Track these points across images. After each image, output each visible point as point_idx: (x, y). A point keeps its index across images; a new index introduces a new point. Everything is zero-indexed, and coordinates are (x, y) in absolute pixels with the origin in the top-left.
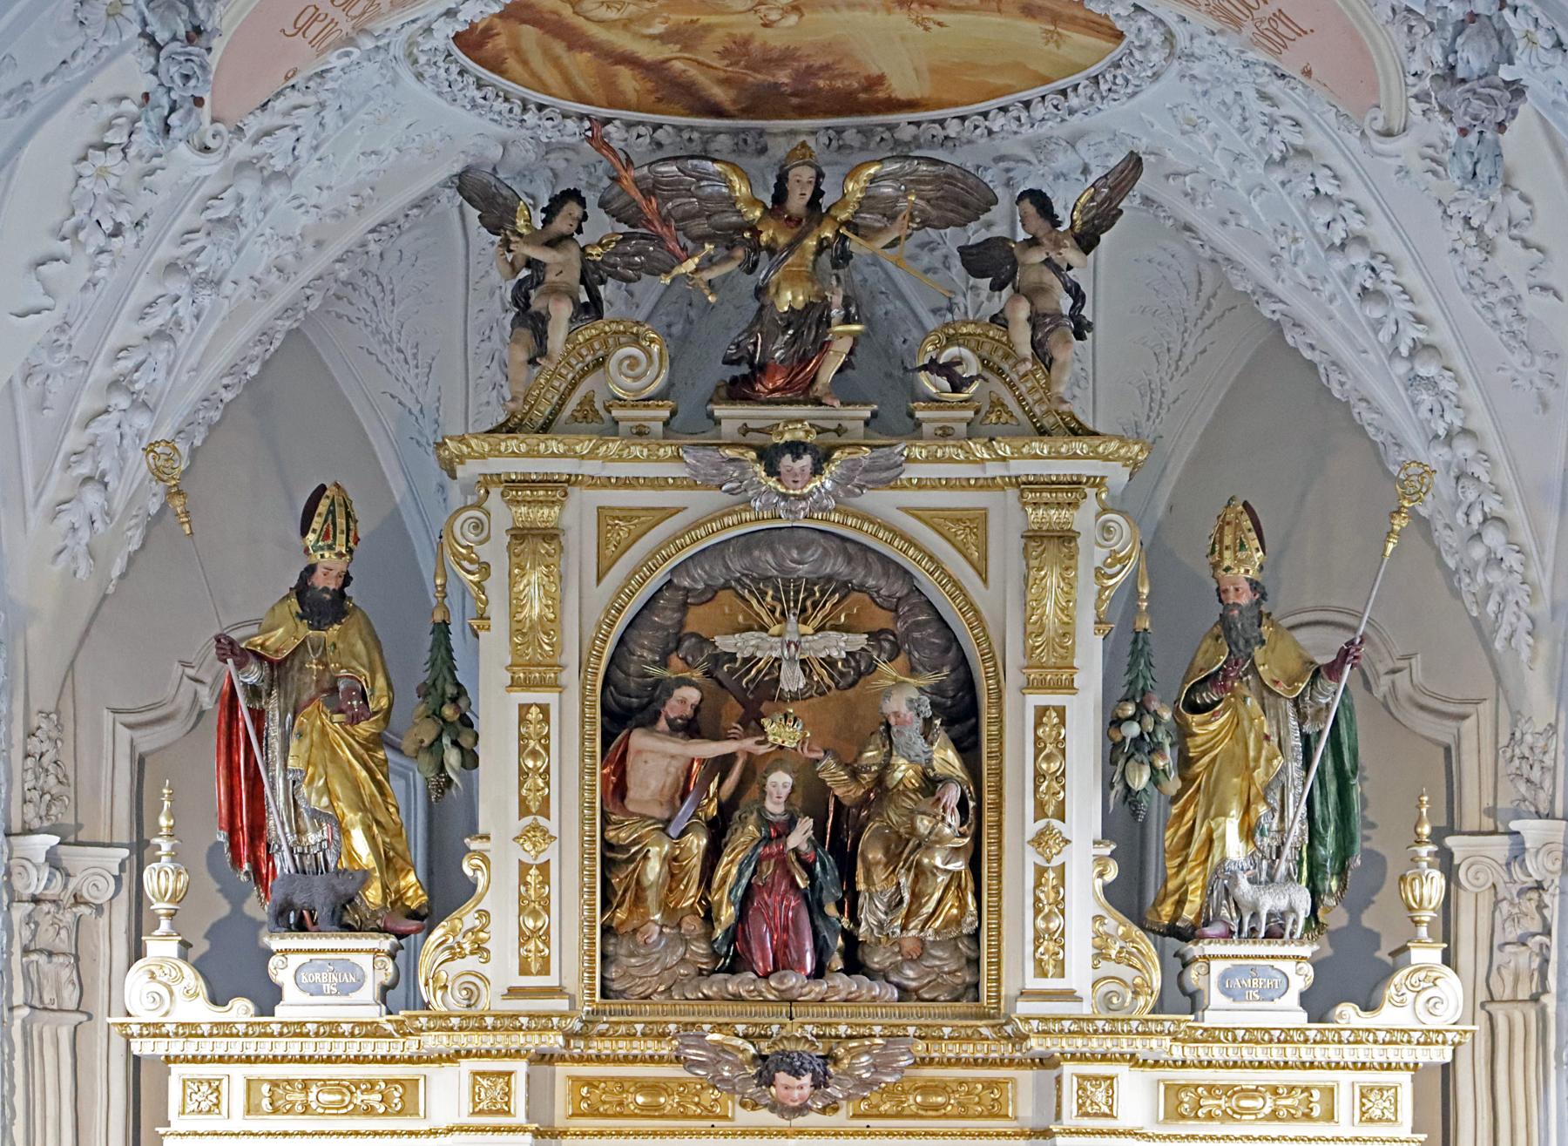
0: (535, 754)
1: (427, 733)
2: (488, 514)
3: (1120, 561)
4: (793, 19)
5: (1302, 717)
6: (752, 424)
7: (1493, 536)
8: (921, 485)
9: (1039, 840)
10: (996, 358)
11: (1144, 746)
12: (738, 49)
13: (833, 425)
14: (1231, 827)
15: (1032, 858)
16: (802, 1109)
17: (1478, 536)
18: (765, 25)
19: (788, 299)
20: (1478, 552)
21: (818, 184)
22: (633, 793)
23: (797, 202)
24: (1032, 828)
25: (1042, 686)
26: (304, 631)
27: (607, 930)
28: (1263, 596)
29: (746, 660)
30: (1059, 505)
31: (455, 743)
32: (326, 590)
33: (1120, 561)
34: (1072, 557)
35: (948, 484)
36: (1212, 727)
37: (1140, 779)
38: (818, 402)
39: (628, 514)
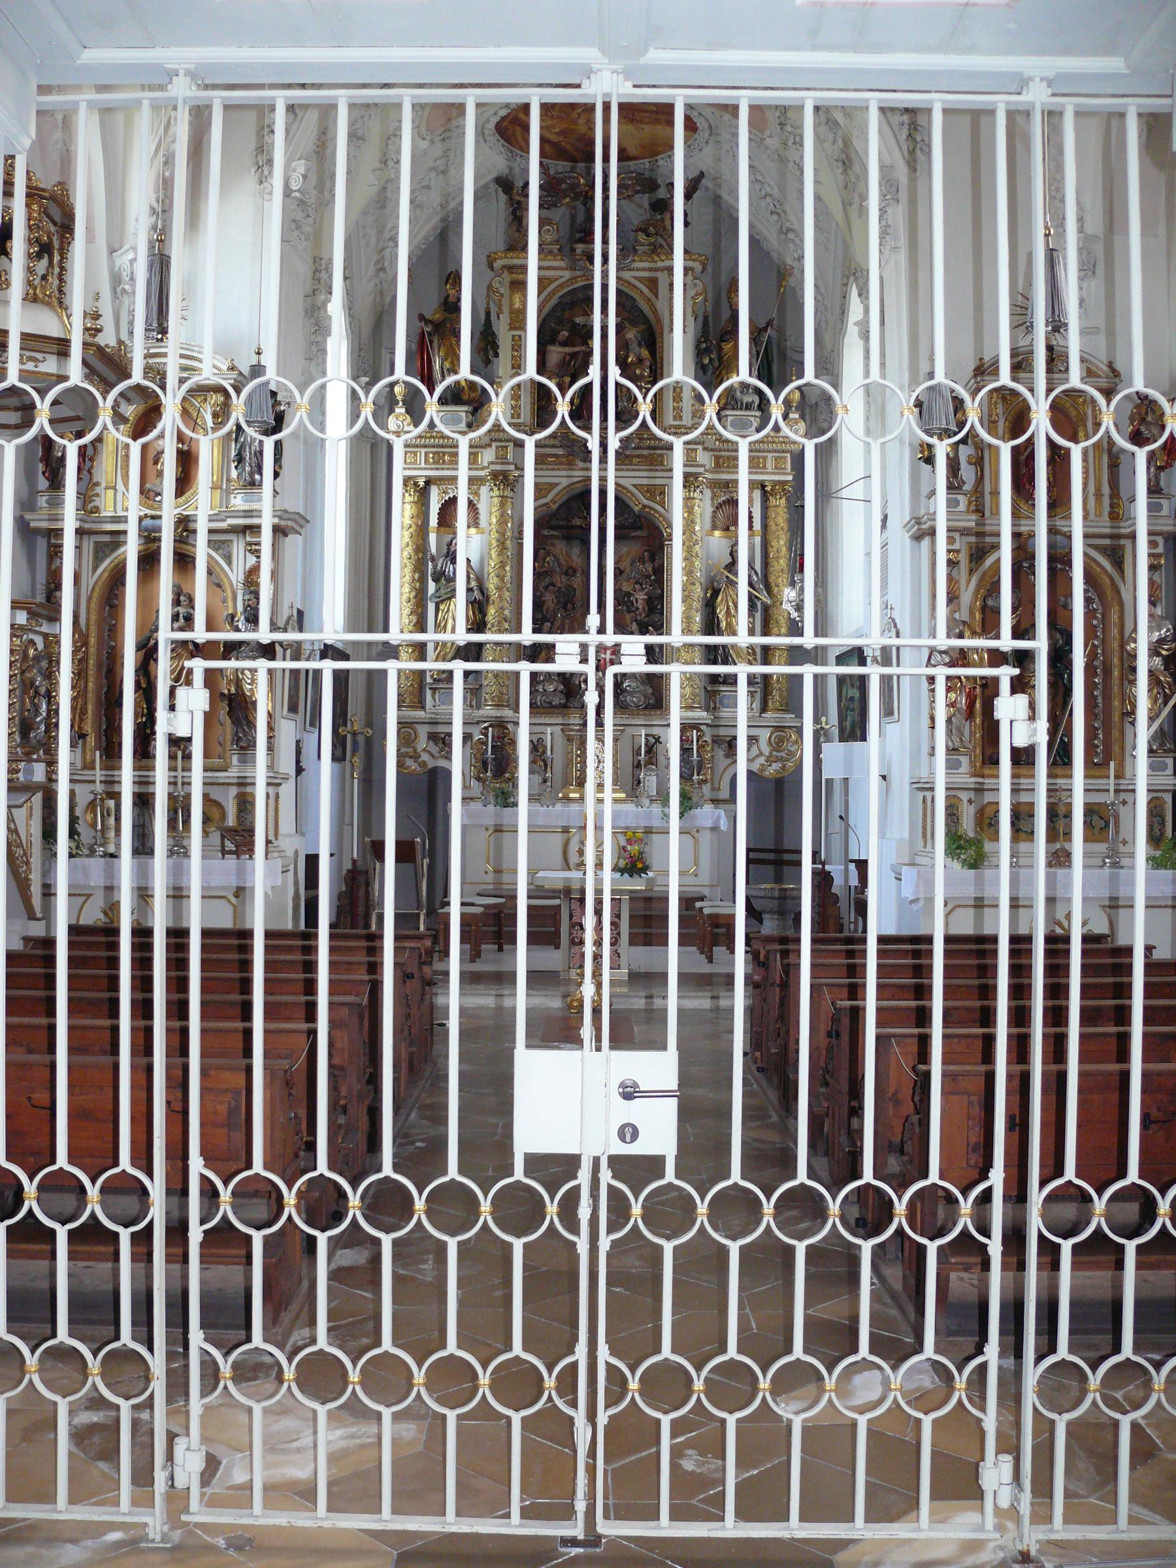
11: (707, 351)
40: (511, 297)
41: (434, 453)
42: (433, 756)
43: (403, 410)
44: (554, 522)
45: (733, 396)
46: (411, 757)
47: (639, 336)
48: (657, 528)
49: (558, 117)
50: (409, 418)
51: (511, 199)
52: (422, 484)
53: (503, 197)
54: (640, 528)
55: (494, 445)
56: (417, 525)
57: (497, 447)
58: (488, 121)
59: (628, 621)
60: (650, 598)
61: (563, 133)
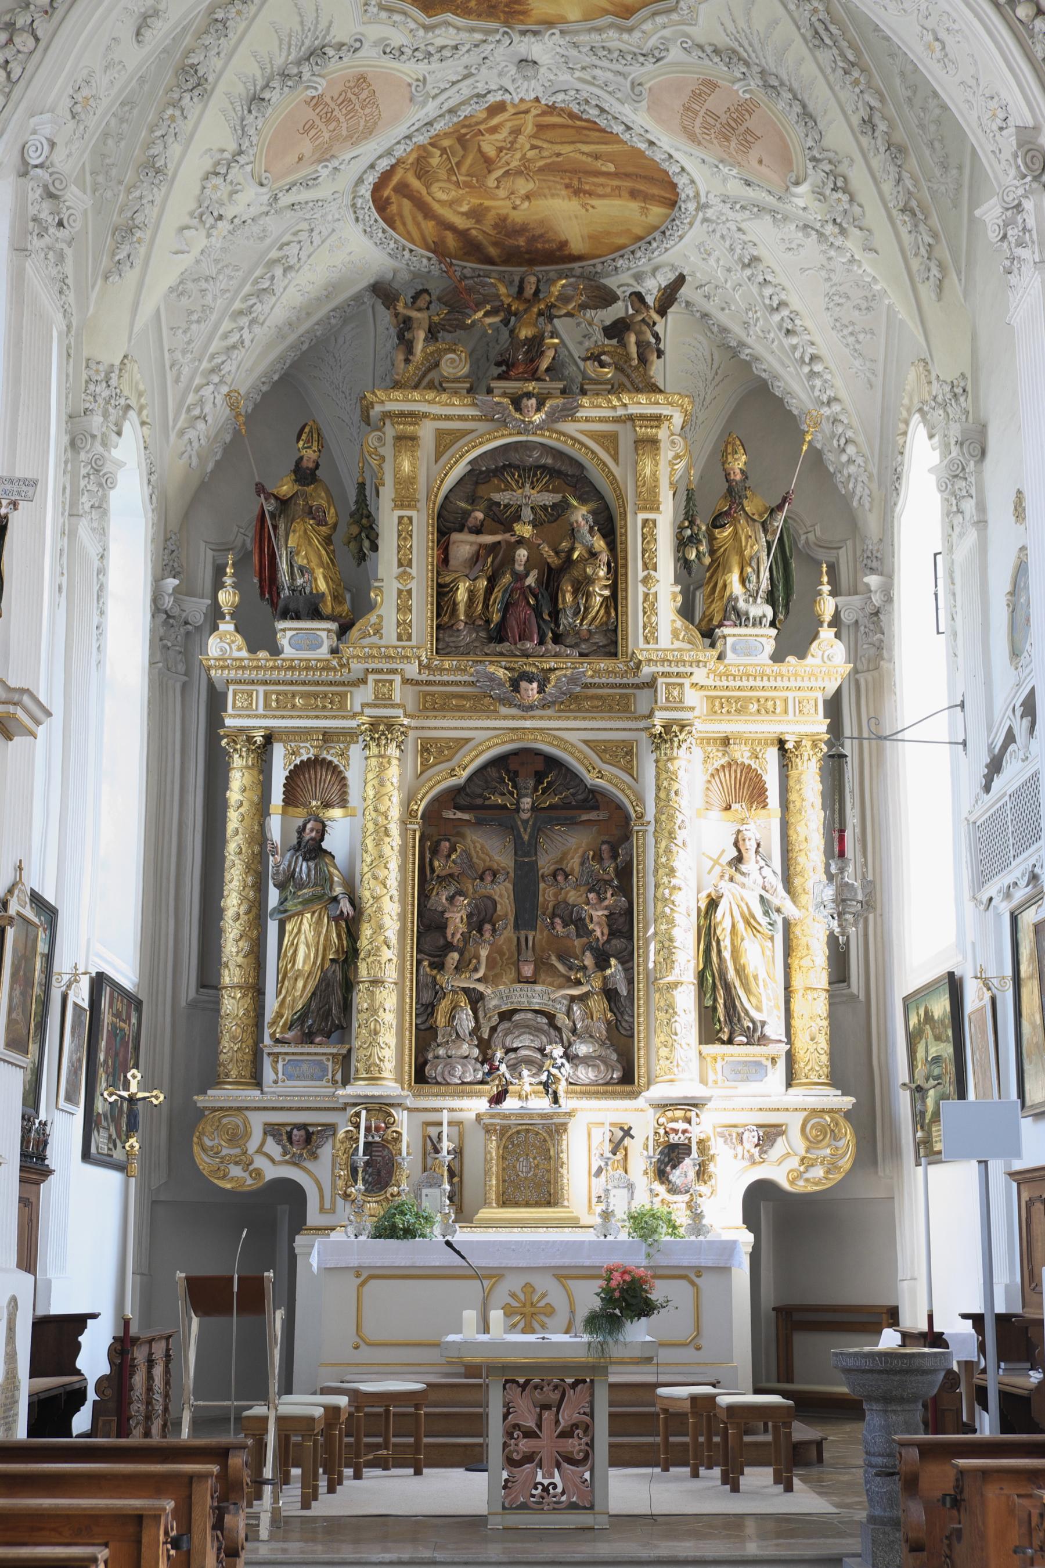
0: (405, 539)
1: (355, 530)
2: (384, 433)
3: (680, 457)
4: (526, 204)
5: (765, 531)
6: (508, 391)
7: (851, 450)
8: (587, 420)
9: (646, 580)
10: (621, 363)
11: (694, 540)
12: (501, 224)
13: (546, 391)
14: (734, 577)
15: (641, 589)
16: (531, 707)
17: (844, 450)
18: (514, 208)
19: (525, 333)
20: (844, 458)
21: (537, 287)
22: (452, 562)
23: (529, 291)
24: (641, 574)
25: (645, 509)
26: (296, 488)
27: (439, 627)
28: (747, 478)
29: (505, 506)
30: (652, 427)
31: (367, 537)
32: (307, 468)
33: (680, 457)
34: (658, 449)
35: (601, 420)
36: (726, 534)
37: (692, 556)
38: (539, 379)
39: (450, 432)
40: (395, 457)
41: (278, 694)
42: (272, 1160)
43: (231, 627)
44: (462, 801)
45: (735, 608)
46: (237, 1163)
47: (590, 518)
48: (619, 807)
49: (467, 185)
50: (239, 640)
51: (396, 315)
52: (259, 740)
53: (385, 317)
54: (596, 808)
55: (371, 678)
56: (252, 802)
57: (377, 681)
58: (360, 181)
59: (578, 951)
60: (611, 914)
61: (476, 214)
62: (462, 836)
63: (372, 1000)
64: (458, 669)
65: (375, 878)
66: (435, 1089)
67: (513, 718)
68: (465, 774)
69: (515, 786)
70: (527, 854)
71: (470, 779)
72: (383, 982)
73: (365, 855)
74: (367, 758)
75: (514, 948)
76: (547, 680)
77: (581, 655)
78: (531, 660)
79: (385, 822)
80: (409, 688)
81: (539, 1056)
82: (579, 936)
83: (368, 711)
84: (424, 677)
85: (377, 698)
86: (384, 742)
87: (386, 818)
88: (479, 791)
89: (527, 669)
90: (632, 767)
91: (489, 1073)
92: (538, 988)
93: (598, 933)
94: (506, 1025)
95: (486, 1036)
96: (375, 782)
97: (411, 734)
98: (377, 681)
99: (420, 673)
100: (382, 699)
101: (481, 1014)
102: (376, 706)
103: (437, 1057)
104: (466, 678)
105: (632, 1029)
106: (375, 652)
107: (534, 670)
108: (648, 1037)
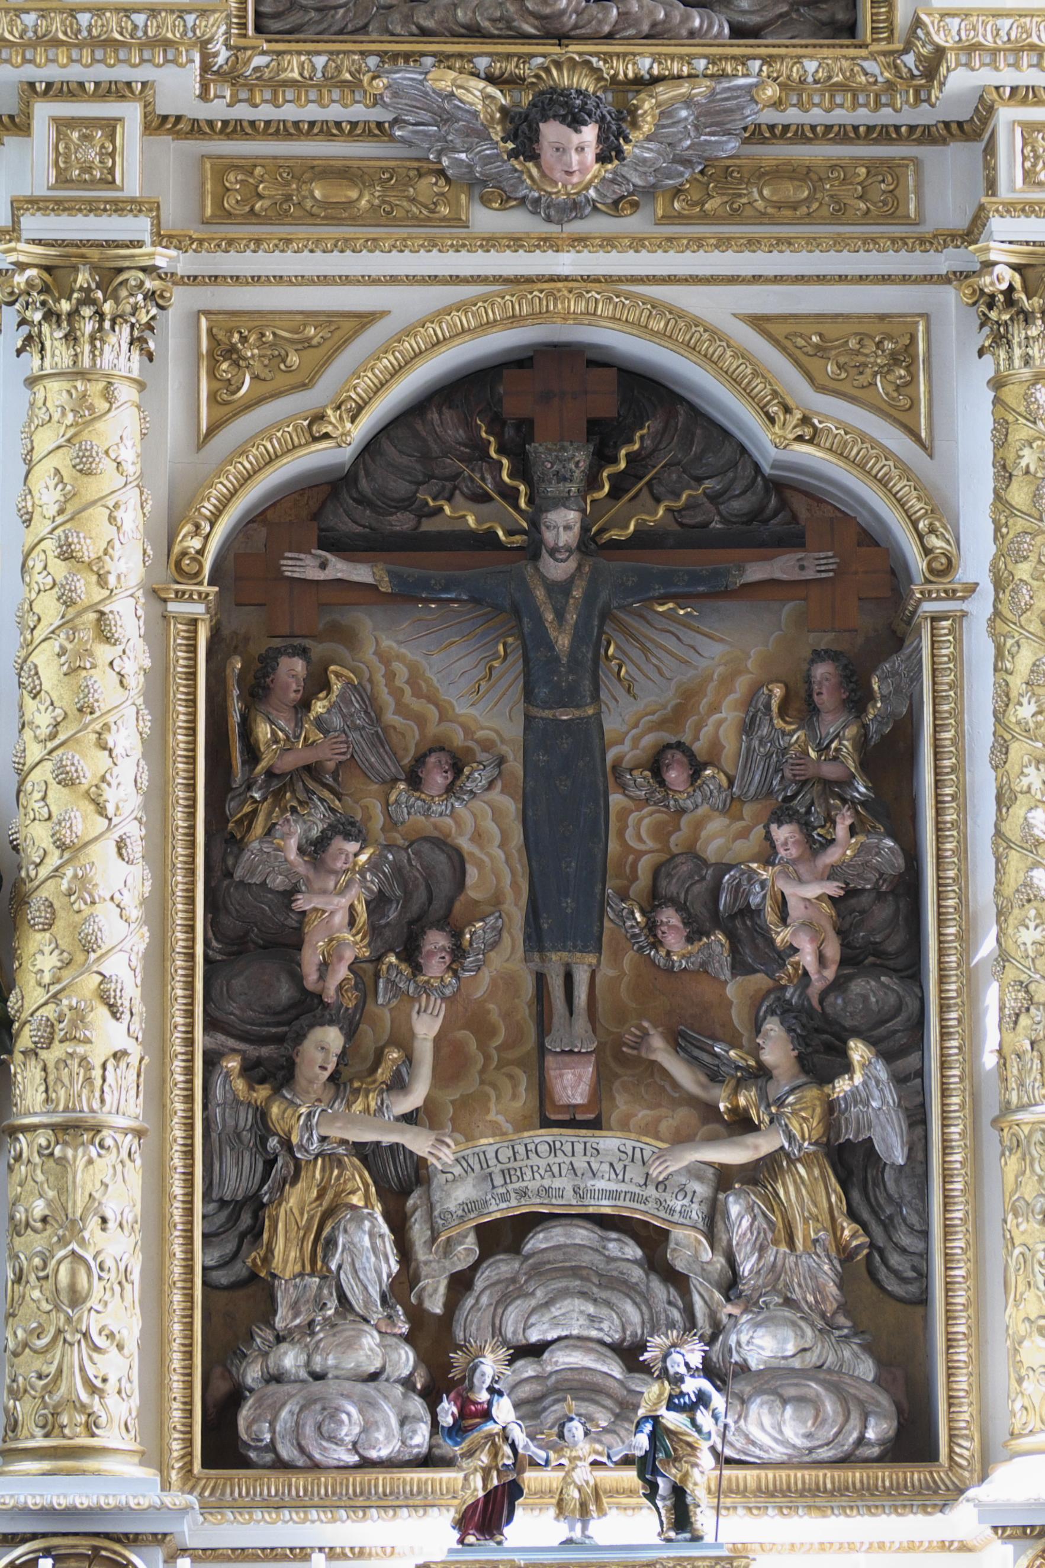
44: (344, 524)
55: (43, 112)
57: (63, 125)
59: (738, 1017)
60: (851, 893)
62: (347, 637)
63: (62, 1190)
64: (331, 81)
65: (67, 780)
66: (273, 1483)
67: (516, 242)
68: (359, 431)
69: (522, 471)
70: (568, 697)
71: (371, 448)
72: (97, 1129)
73: (30, 704)
74: (32, 382)
75: (525, 1012)
76: (627, 116)
77: (739, 32)
78: (574, 49)
79: (101, 594)
80: (167, 145)
81: (615, 1369)
82: (740, 967)
83: (33, 224)
84: (218, 110)
85: (63, 180)
86: (89, 327)
87: (102, 580)
88: (400, 487)
89: (564, 79)
90: (914, 404)
91: (458, 1431)
92: (609, 1142)
93: (807, 958)
94: (502, 1267)
95: (436, 1306)
96: (63, 460)
97: (181, 299)
98: (63, 125)
99: (204, 96)
100: (82, 184)
101: (419, 1232)
102: (60, 206)
103: (276, 1378)
104: (359, 112)
105: (923, 1276)
106: (57, 26)
107: (587, 84)
108: (978, 1302)
